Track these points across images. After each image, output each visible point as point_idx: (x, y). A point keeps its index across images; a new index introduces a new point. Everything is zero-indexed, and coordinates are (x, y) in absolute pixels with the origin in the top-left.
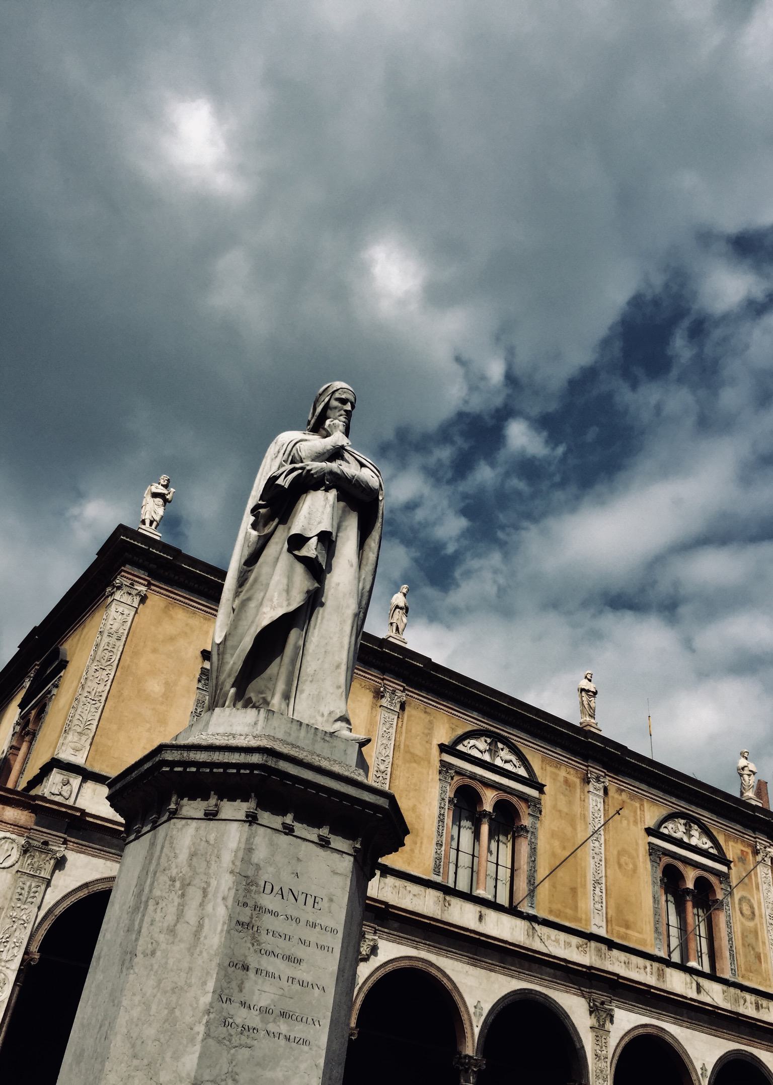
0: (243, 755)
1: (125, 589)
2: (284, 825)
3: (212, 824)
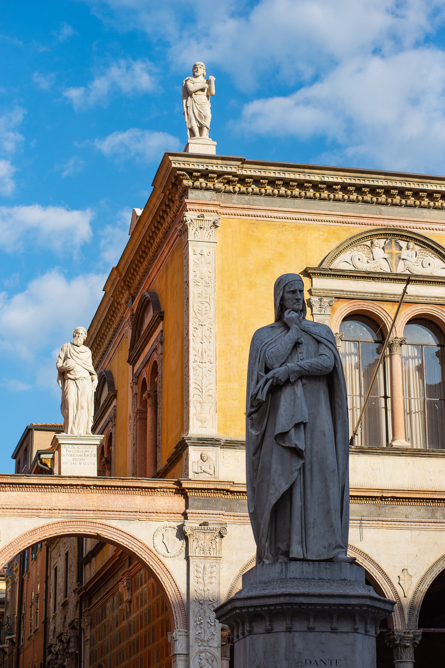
0: (275, 598)
1: (197, 224)
2: (308, 627)
3: (270, 634)
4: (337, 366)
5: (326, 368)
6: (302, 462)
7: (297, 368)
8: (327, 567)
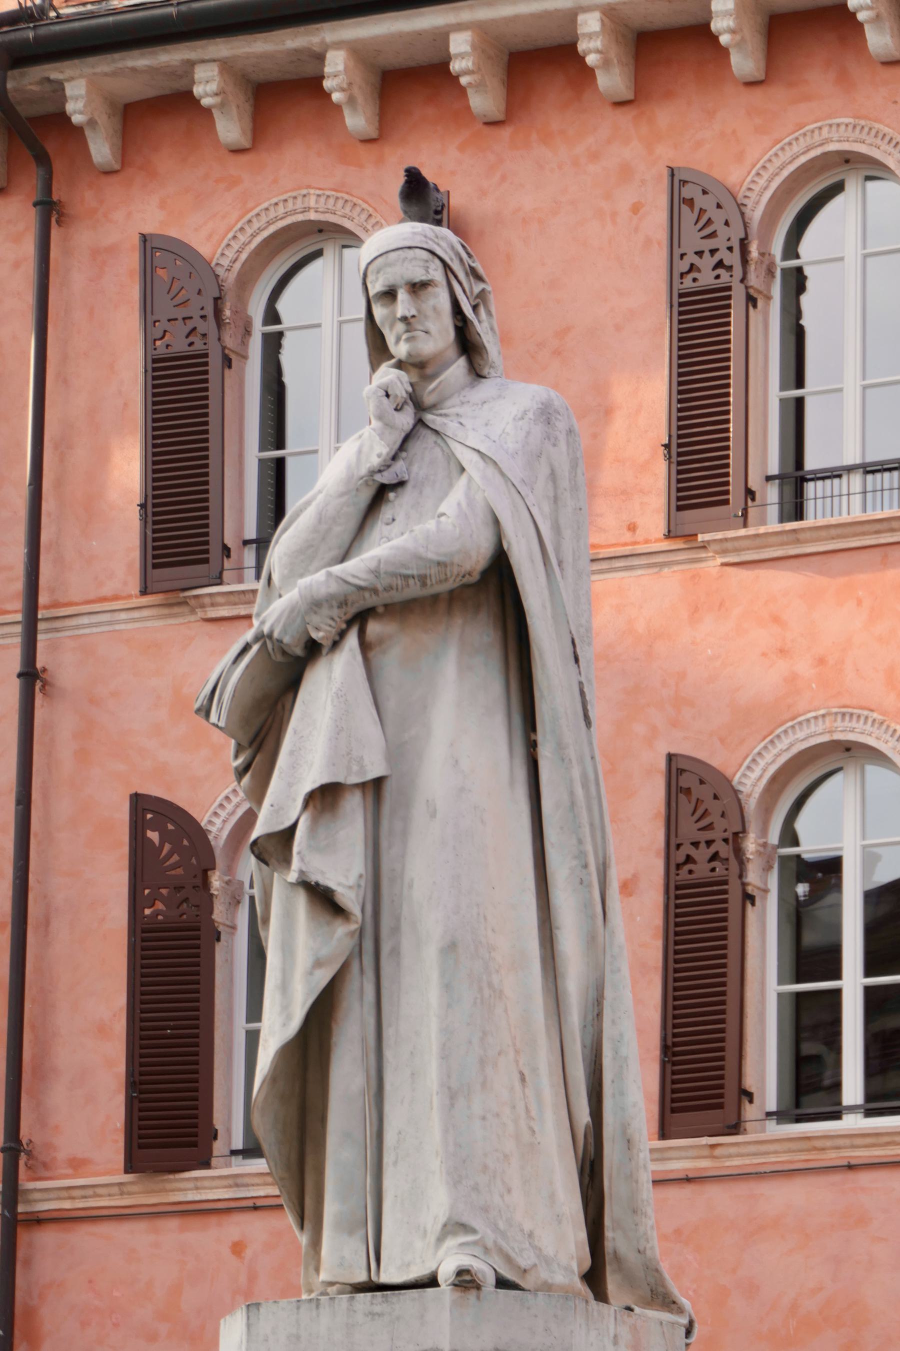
4: (505, 547)
5: (439, 563)
6: (341, 930)
7: (333, 588)
8: (377, 1309)
